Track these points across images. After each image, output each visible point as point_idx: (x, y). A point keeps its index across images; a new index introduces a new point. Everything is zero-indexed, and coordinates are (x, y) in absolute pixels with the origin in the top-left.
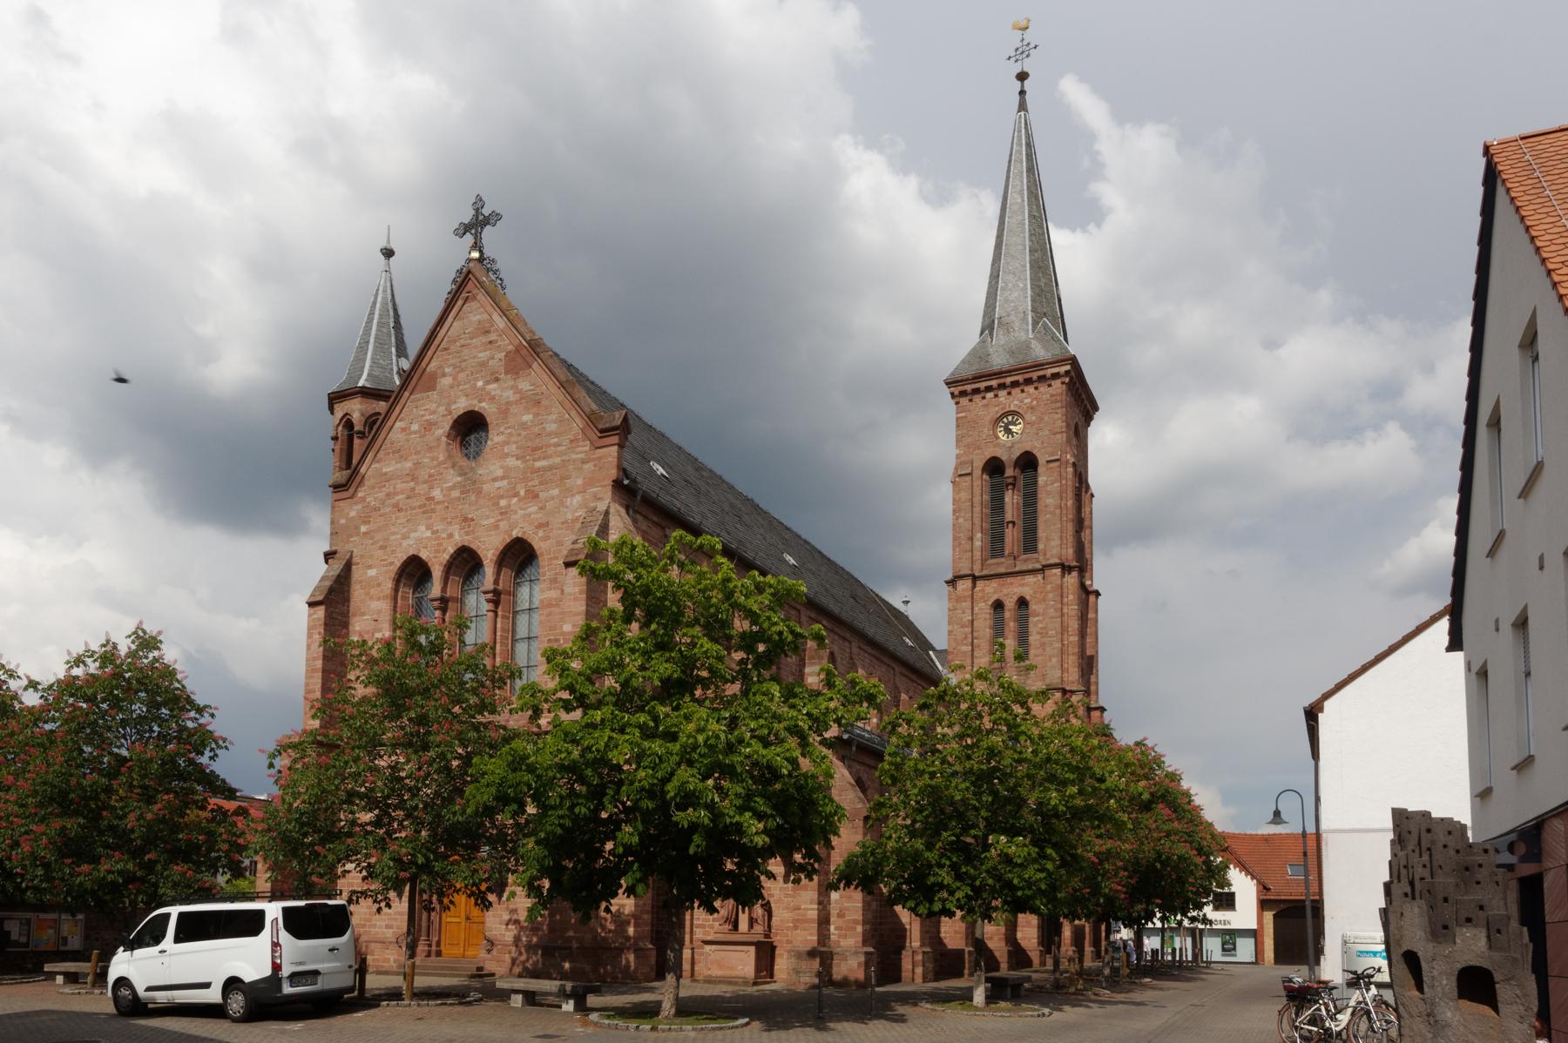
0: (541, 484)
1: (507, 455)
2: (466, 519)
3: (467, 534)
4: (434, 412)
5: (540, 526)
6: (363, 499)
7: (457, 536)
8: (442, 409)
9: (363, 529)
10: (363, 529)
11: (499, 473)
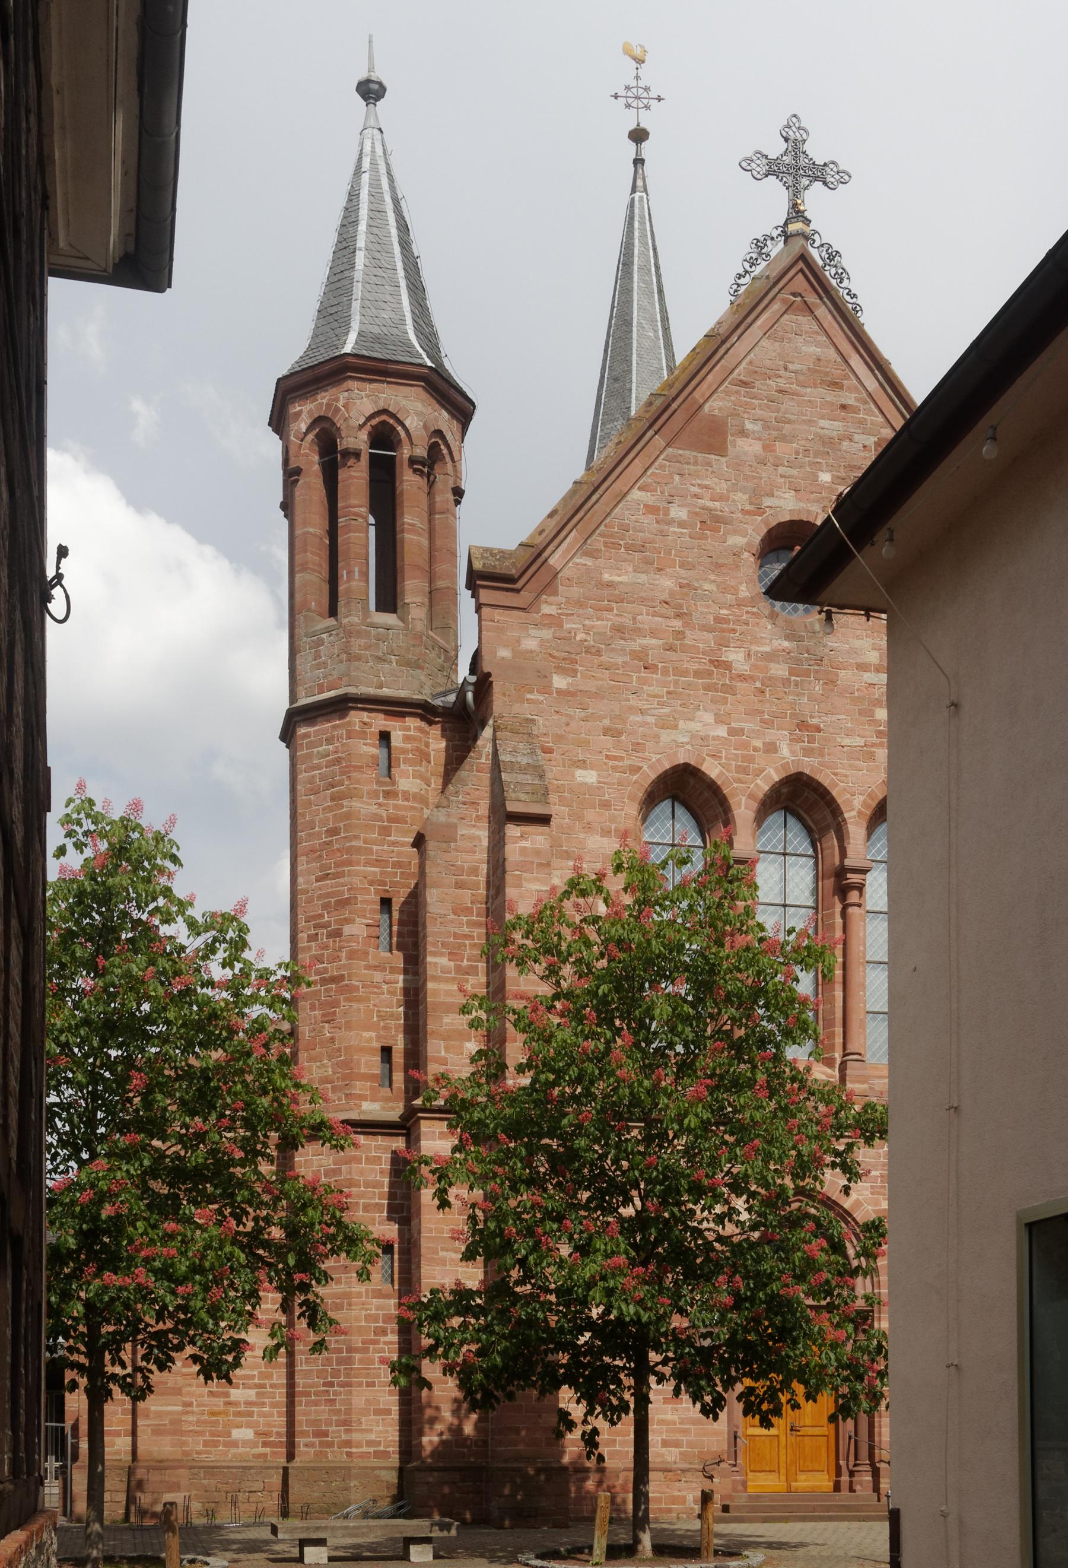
4: (721, 498)
8: (741, 499)
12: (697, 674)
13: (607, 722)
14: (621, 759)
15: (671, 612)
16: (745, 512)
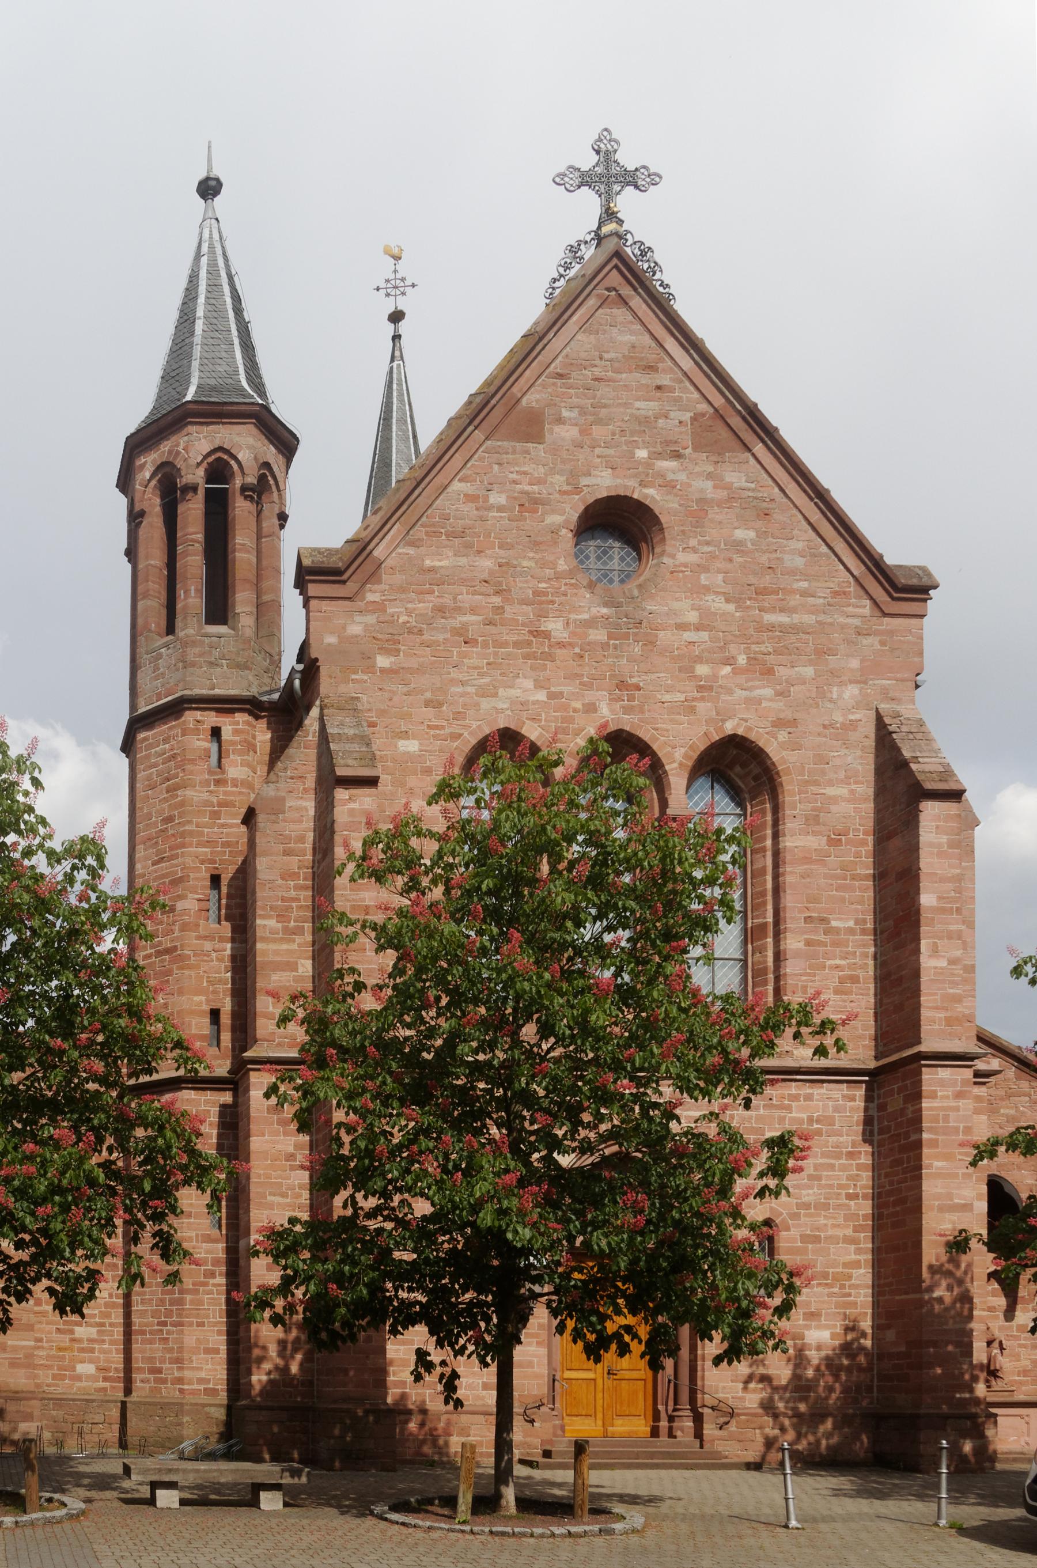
2: (622, 685)
5: (780, 723)
10: (383, 661)
12: (517, 644)
14: (443, 727)
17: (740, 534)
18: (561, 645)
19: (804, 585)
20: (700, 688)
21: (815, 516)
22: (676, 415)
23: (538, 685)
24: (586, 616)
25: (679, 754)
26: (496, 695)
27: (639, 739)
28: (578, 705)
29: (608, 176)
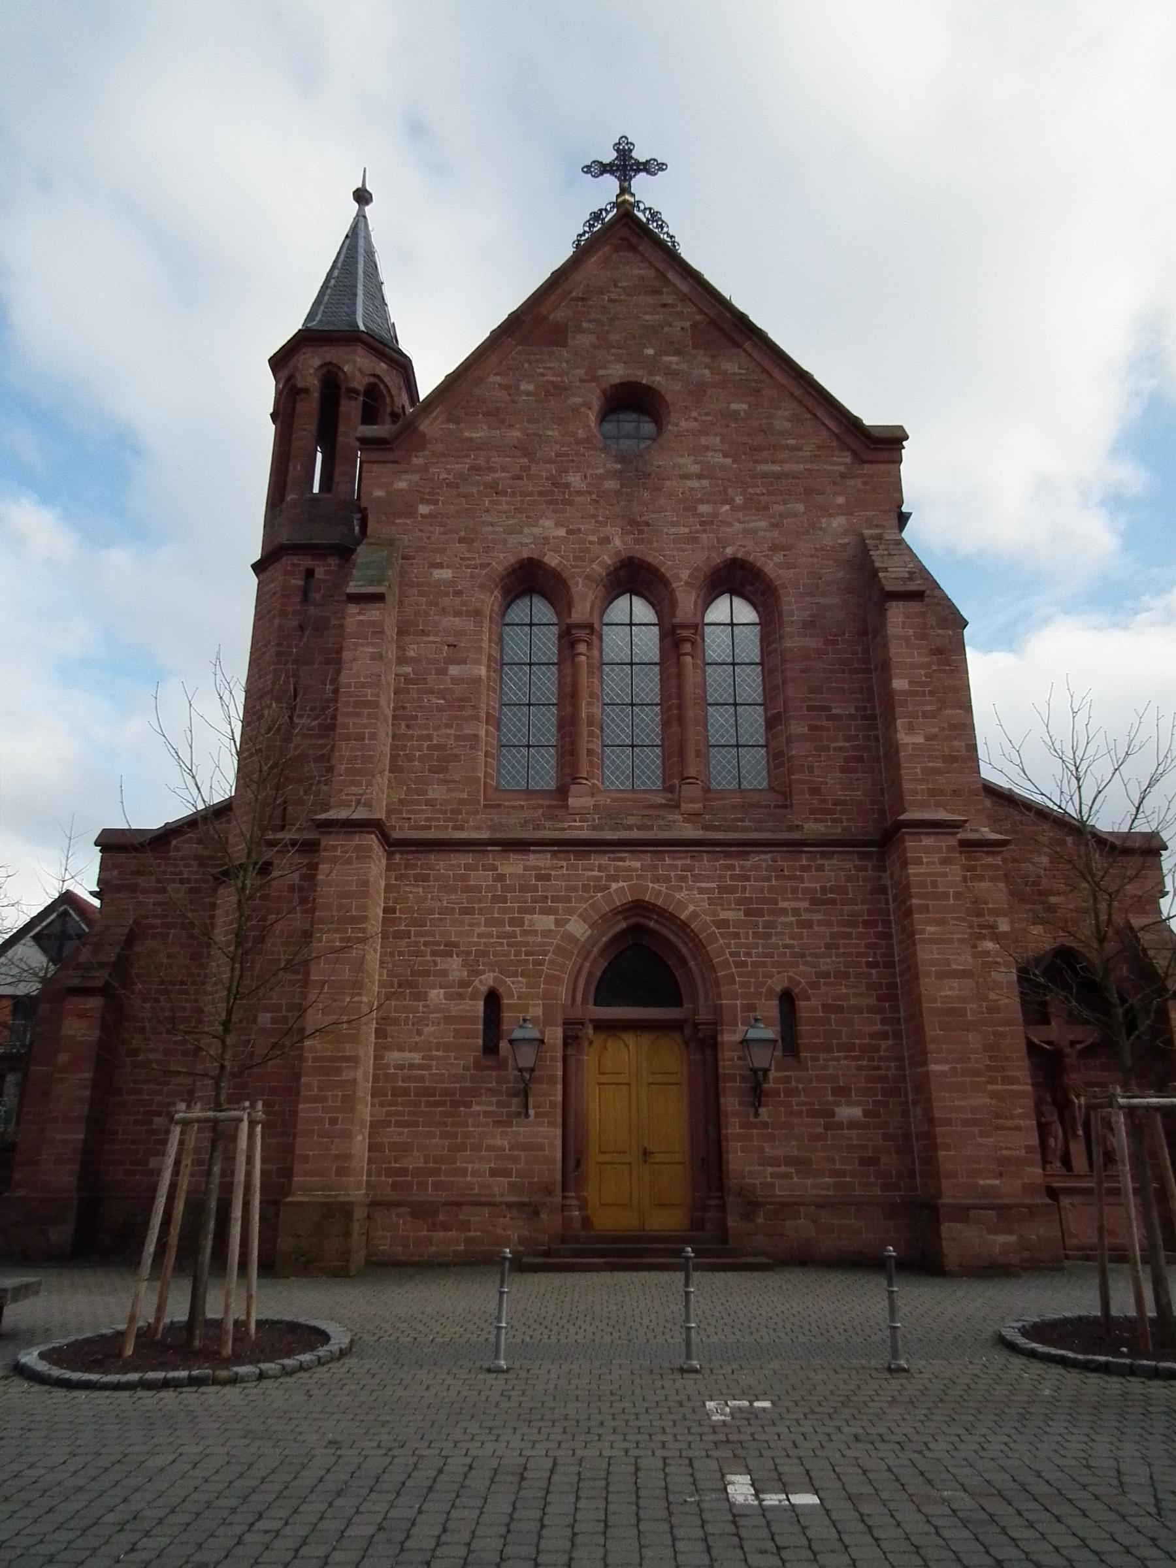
0: (770, 493)
1: (707, 448)
2: (632, 522)
3: (637, 541)
5: (775, 548)
6: (425, 469)
7: (617, 542)
9: (423, 509)
10: (423, 509)
11: (695, 469)
12: (540, 493)
13: (462, 534)
14: (474, 559)
15: (517, 453)
16: (581, 381)
17: (734, 406)
18: (579, 493)
19: (793, 442)
20: (702, 523)
21: (798, 392)
22: (678, 324)
23: (558, 524)
24: (601, 471)
25: (685, 574)
26: (521, 532)
27: (649, 564)
28: (594, 538)
29: (625, 165)
